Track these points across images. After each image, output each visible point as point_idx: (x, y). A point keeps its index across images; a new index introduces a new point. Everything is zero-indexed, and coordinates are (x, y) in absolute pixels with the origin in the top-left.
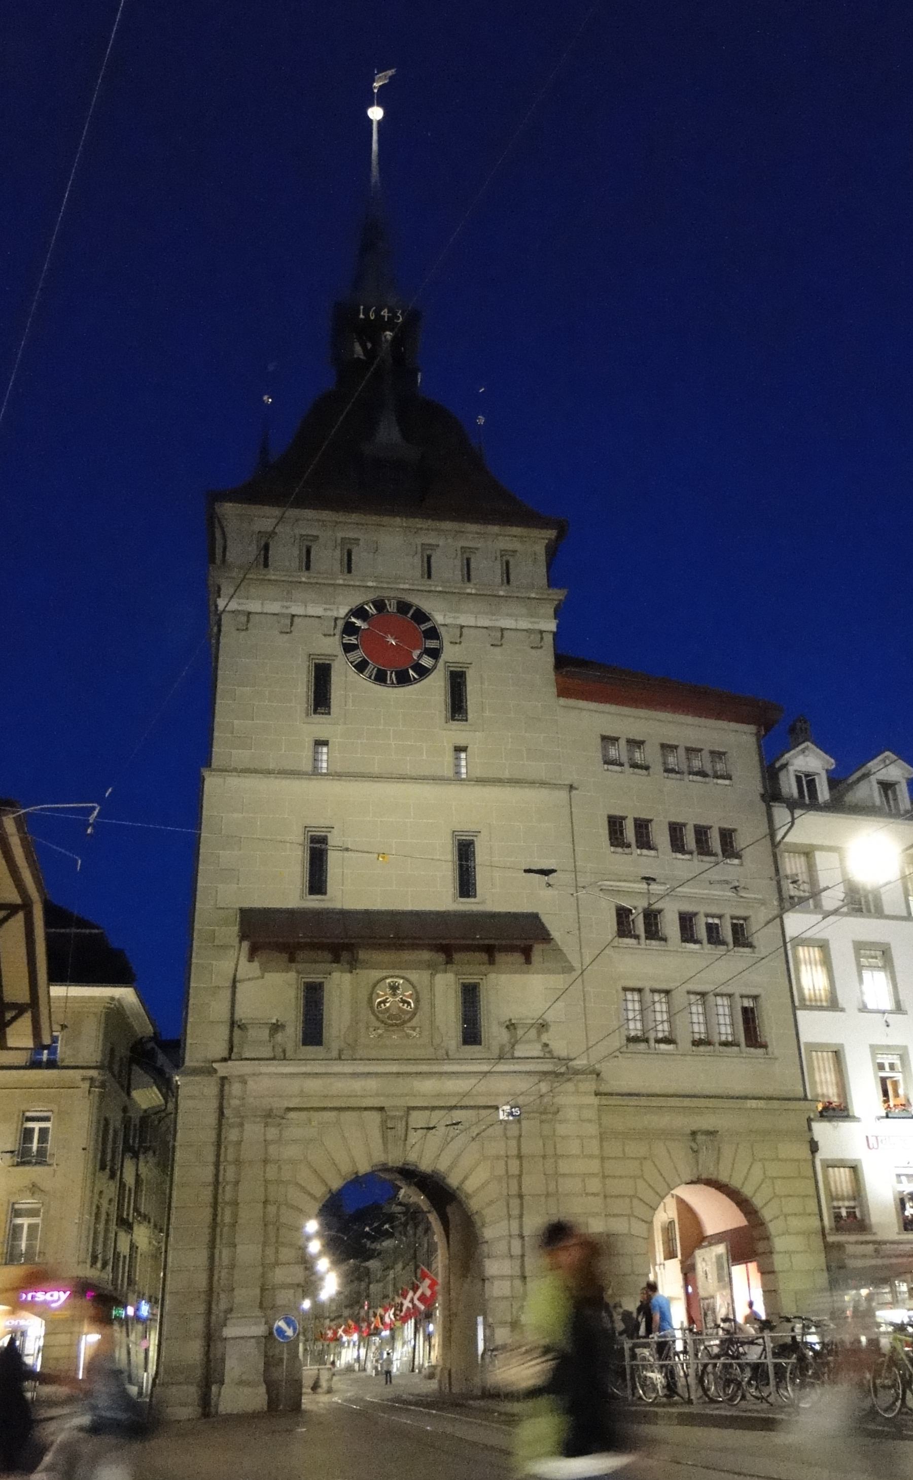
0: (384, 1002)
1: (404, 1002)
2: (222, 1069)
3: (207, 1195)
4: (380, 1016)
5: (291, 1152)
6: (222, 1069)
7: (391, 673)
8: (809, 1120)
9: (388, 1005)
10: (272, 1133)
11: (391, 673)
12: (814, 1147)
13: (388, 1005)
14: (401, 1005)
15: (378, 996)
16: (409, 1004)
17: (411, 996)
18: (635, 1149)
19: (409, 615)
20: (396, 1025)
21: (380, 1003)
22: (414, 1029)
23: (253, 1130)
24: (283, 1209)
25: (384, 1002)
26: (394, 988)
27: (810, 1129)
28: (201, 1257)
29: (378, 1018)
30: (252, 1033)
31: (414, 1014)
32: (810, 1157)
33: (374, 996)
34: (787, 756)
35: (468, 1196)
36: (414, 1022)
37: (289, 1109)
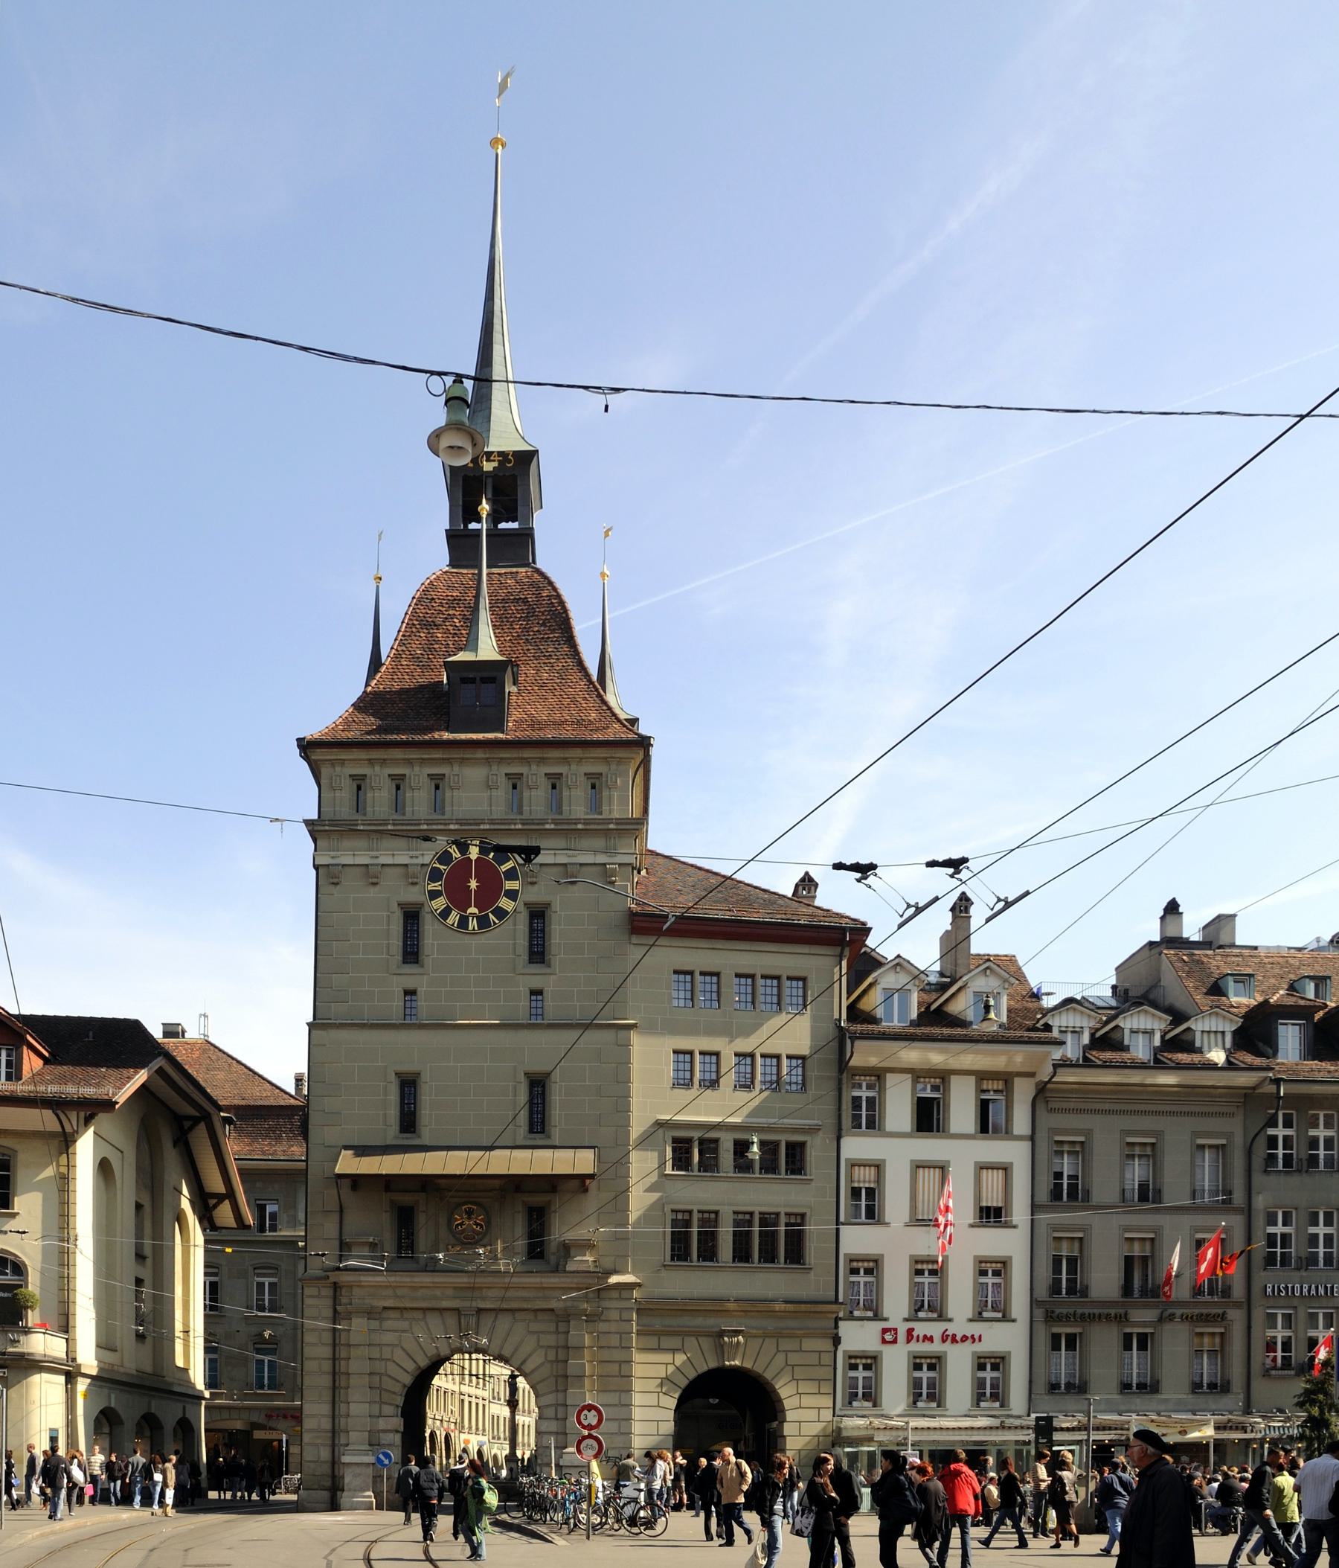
1: (477, 1224)
2: (334, 1277)
3: (327, 1366)
5: (388, 1338)
6: (334, 1277)
8: (837, 1320)
10: (375, 1324)
12: (837, 1341)
23: (358, 1326)
24: (384, 1378)
25: (461, 1224)
26: (469, 1213)
27: (836, 1327)
28: (325, 1409)
31: (485, 1234)
32: (832, 1349)
34: (874, 975)
37: (385, 1308)
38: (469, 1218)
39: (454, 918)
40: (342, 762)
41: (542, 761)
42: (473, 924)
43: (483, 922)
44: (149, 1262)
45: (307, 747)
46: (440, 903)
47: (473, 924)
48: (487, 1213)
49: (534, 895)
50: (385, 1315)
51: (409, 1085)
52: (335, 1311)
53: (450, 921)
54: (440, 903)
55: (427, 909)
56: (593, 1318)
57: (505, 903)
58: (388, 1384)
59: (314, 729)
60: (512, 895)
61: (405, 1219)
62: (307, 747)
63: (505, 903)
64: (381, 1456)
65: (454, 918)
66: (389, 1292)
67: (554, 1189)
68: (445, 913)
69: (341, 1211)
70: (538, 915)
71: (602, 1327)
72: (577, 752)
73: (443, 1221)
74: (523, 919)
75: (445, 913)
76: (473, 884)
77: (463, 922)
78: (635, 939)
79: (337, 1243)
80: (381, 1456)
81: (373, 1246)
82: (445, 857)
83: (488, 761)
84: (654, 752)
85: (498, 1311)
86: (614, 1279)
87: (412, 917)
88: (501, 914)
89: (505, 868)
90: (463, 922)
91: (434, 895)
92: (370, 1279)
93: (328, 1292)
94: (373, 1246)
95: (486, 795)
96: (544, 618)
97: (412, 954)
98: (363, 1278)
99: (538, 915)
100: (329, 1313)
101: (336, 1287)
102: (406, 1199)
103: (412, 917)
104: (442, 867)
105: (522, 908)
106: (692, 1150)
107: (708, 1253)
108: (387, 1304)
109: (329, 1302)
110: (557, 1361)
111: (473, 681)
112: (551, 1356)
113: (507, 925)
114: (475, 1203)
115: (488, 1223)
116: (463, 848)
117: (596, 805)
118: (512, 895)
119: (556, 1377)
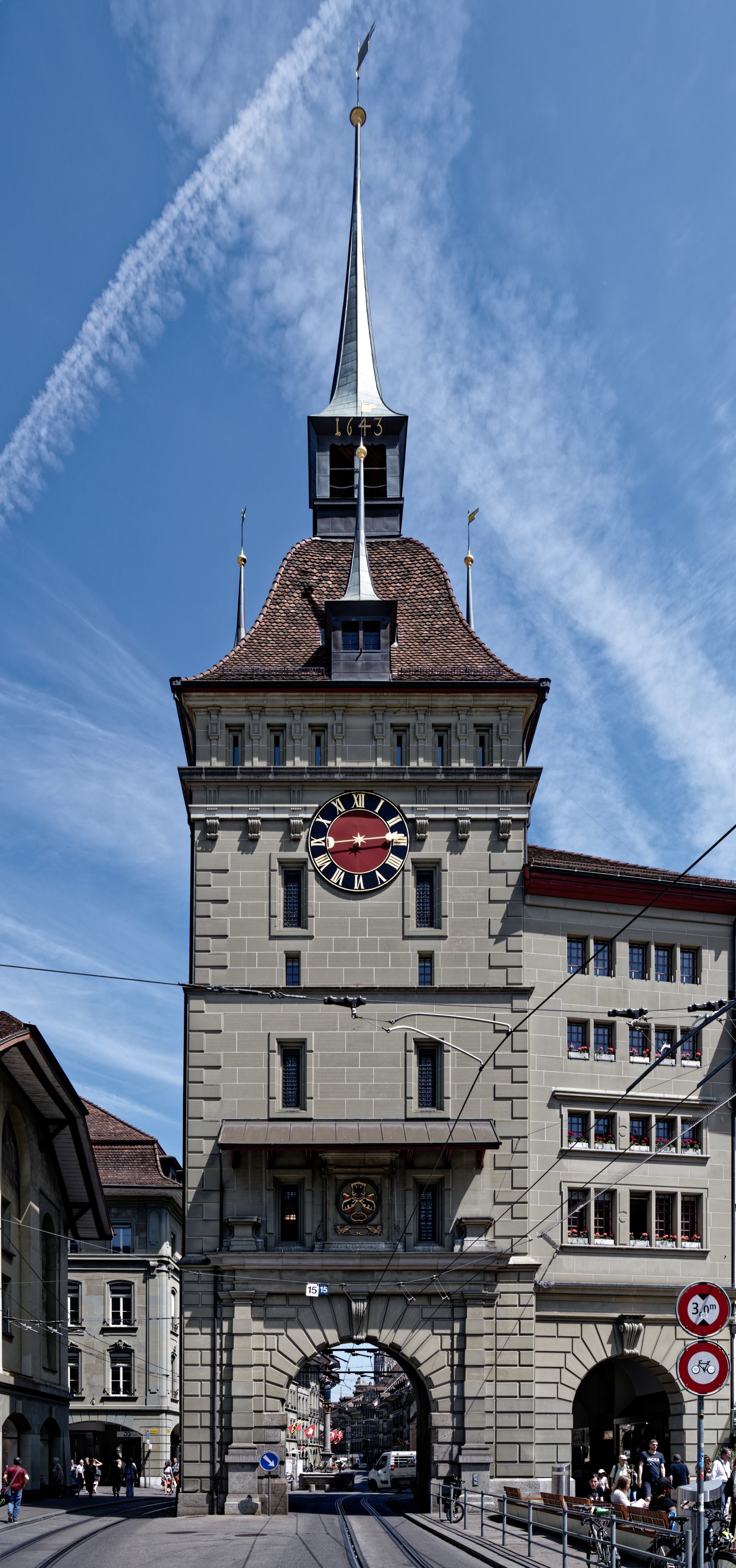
0: (350, 1203)
1: (367, 1203)
4: (347, 1215)
7: (358, 878)
9: (353, 1206)
11: (358, 878)
13: (353, 1206)
14: (364, 1205)
15: (345, 1198)
16: (371, 1205)
17: (372, 1198)
18: (572, 1329)
19: (382, 802)
20: (360, 1223)
21: (345, 1205)
22: (376, 1226)
25: (350, 1203)
26: (359, 1190)
29: (343, 1217)
30: (238, 1231)
31: (376, 1213)
33: (341, 1198)
35: (419, 1365)
36: (375, 1222)
37: (270, 1294)
38: (358, 1196)
39: (338, 877)
40: (219, 710)
41: (430, 710)
42: (359, 883)
43: (370, 880)
44: (16, 1260)
47: (359, 883)
48: (377, 1189)
50: (269, 1301)
52: (216, 1298)
53: (334, 879)
54: (323, 861)
55: (310, 867)
56: (490, 1301)
57: (394, 861)
58: (273, 1375)
60: (400, 852)
61: (288, 1199)
63: (394, 861)
64: (266, 1458)
65: (338, 877)
66: (273, 1277)
67: (447, 1165)
68: (330, 871)
69: (222, 1190)
71: (502, 1312)
72: (466, 699)
73: (331, 1199)
74: (410, 878)
75: (330, 871)
76: (359, 839)
77: (349, 880)
78: (529, 900)
79: (217, 1224)
80: (266, 1458)
81: (256, 1227)
82: (329, 812)
83: (373, 711)
85: (389, 1296)
86: (513, 1260)
88: (388, 871)
89: (392, 822)
90: (349, 880)
91: (318, 851)
92: (255, 1261)
93: (208, 1276)
94: (256, 1227)
95: (371, 746)
97: (296, 913)
98: (248, 1261)
100: (209, 1299)
101: (216, 1270)
102: (290, 1176)
104: (325, 822)
105: (409, 866)
106: (589, 1120)
107: (607, 1229)
108: (272, 1289)
109: (210, 1288)
110: (452, 1350)
112: (447, 1345)
113: (397, 885)
114: (362, 1180)
115: (379, 1202)
116: (348, 801)
117: (486, 758)
118: (400, 852)
119: (452, 1366)
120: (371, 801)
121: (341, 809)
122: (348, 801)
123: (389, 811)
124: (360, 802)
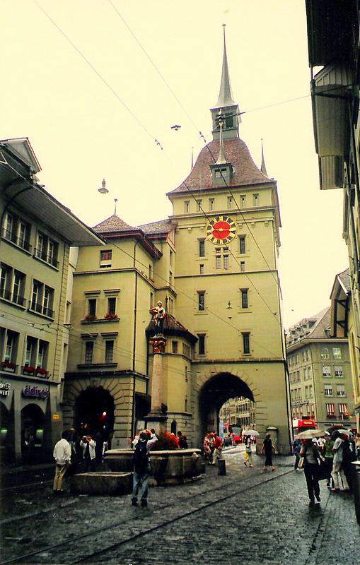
39: (215, 240)
45: (168, 194)
46: (211, 236)
49: (241, 232)
51: (201, 294)
54: (211, 236)
57: (232, 235)
59: (170, 190)
60: (234, 232)
62: (168, 194)
63: (232, 235)
68: (213, 238)
70: (242, 239)
75: (213, 238)
82: (212, 223)
84: (277, 184)
87: (202, 242)
88: (230, 238)
91: (209, 234)
96: (241, 151)
99: (242, 239)
103: (202, 242)
111: (219, 170)
116: (218, 219)
118: (234, 232)
120: (225, 219)
121: (215, 221)
122: (218, 219)
123: (230, 221)
124: (221, 219)
